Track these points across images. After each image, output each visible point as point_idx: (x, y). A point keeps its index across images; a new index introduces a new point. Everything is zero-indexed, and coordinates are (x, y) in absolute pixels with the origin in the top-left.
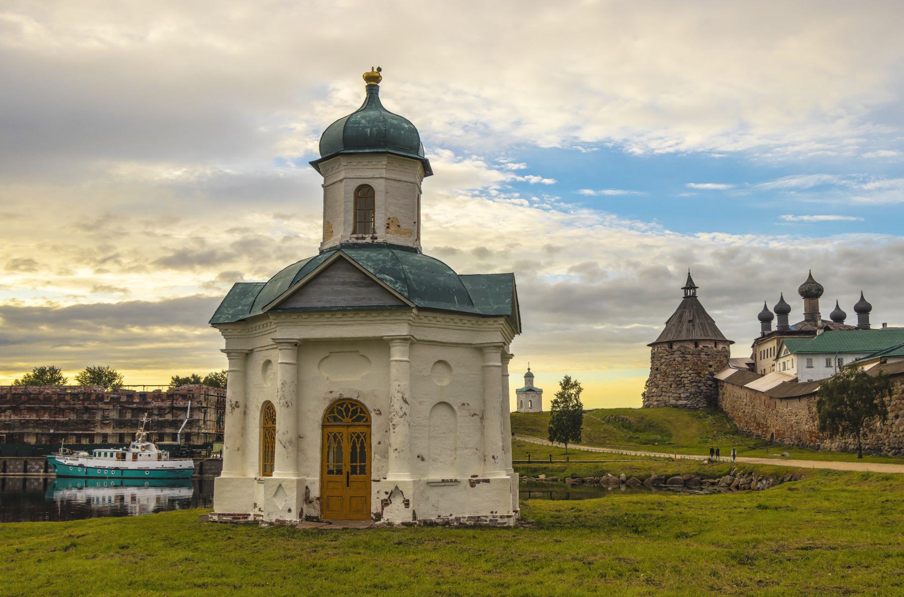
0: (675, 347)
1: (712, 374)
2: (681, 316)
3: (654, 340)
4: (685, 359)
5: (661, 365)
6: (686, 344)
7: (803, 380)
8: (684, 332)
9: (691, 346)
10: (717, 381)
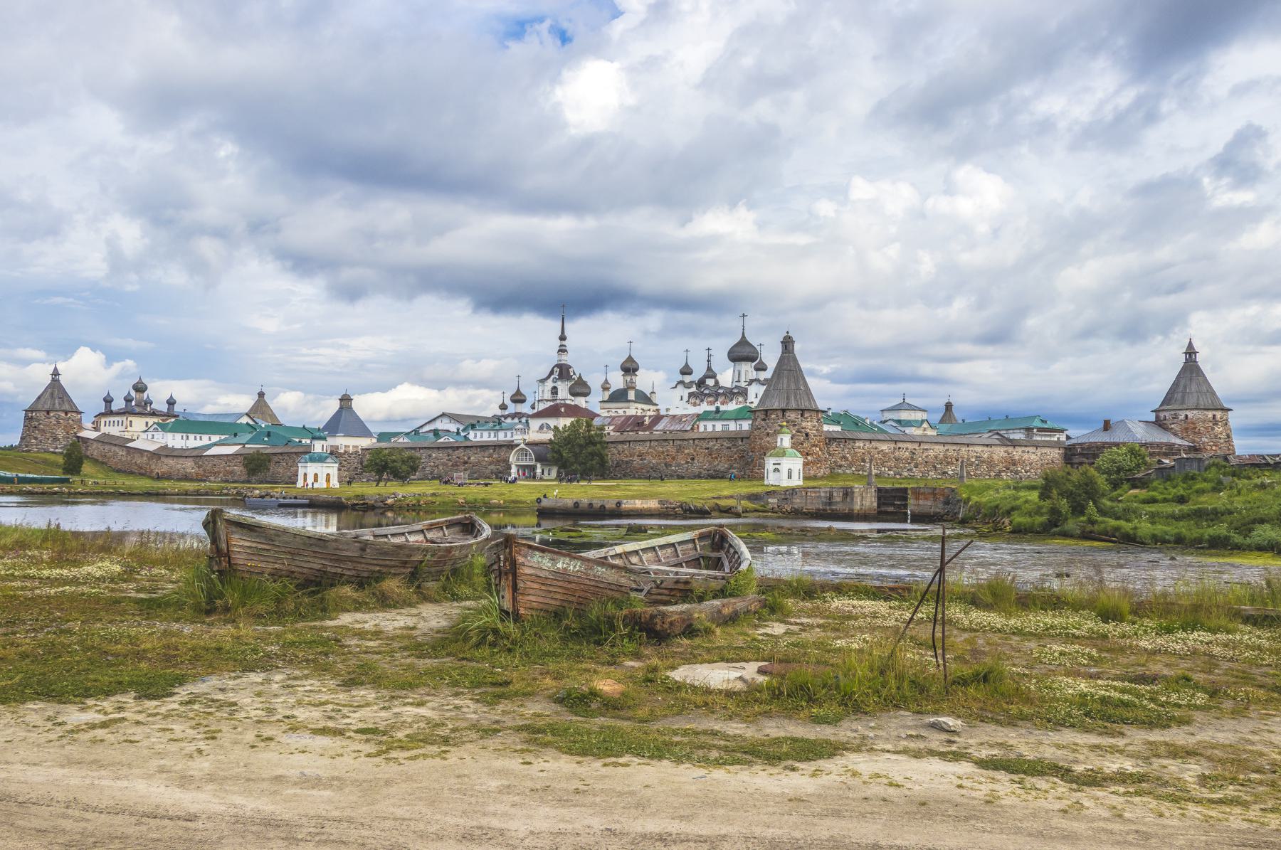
0: (52, 415)
1: (75, 433)
2: (52, 394)
3: (27, 408)
4: (59, 423)
5: (40, 424)
6: (60, 413)
7: (170, 446)
8: (57, 405)
9: (63, 415)
10: (78, 437)
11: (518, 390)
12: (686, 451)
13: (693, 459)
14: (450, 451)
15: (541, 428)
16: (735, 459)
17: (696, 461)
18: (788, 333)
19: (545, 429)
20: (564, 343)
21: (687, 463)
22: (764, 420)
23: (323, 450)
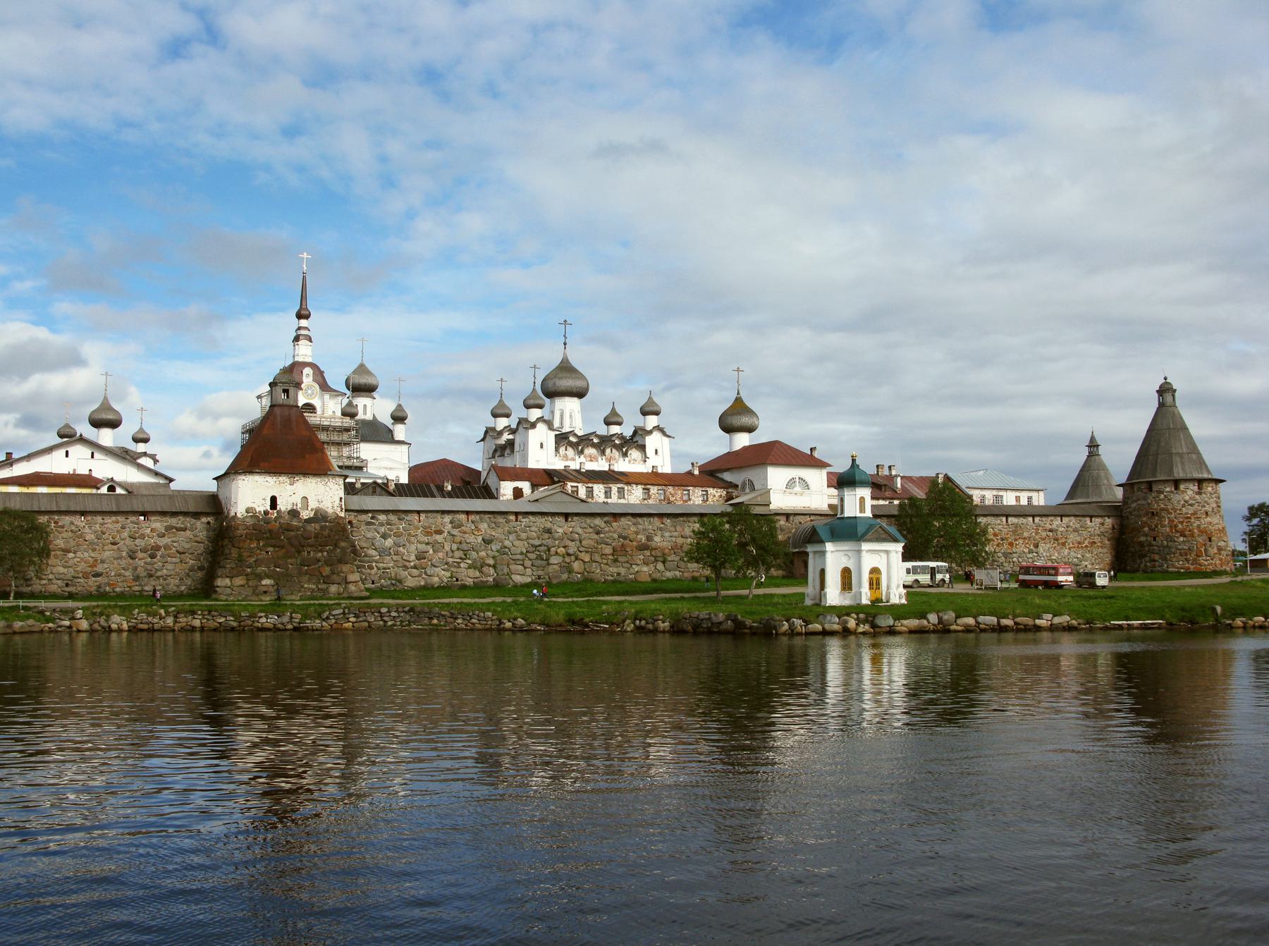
11: (613, 409)
12: (1026, 534)
13: (1036, 546)
14: (598, 522)
15: (791, 484)
16: (1086, 546)
17: (1041, 550)
18: (1165, 379)
19: (798, 489)
20: (304, 323)
21: (1031, 552)
22: (1199, 493)
23: (862, 510)
